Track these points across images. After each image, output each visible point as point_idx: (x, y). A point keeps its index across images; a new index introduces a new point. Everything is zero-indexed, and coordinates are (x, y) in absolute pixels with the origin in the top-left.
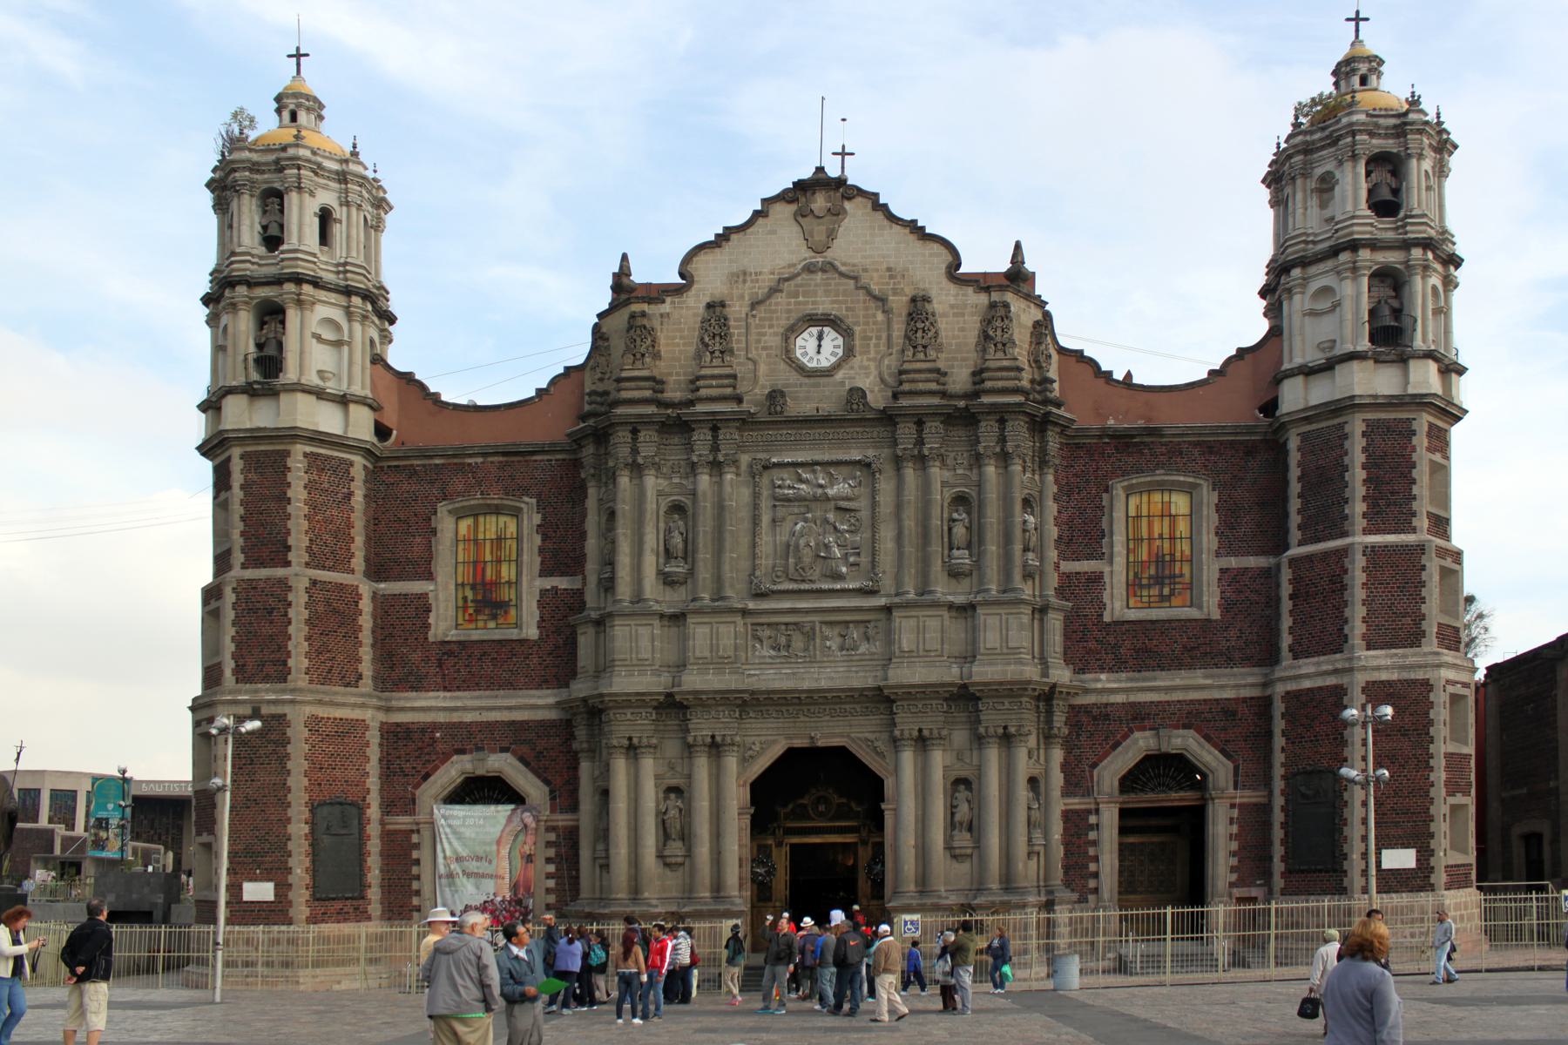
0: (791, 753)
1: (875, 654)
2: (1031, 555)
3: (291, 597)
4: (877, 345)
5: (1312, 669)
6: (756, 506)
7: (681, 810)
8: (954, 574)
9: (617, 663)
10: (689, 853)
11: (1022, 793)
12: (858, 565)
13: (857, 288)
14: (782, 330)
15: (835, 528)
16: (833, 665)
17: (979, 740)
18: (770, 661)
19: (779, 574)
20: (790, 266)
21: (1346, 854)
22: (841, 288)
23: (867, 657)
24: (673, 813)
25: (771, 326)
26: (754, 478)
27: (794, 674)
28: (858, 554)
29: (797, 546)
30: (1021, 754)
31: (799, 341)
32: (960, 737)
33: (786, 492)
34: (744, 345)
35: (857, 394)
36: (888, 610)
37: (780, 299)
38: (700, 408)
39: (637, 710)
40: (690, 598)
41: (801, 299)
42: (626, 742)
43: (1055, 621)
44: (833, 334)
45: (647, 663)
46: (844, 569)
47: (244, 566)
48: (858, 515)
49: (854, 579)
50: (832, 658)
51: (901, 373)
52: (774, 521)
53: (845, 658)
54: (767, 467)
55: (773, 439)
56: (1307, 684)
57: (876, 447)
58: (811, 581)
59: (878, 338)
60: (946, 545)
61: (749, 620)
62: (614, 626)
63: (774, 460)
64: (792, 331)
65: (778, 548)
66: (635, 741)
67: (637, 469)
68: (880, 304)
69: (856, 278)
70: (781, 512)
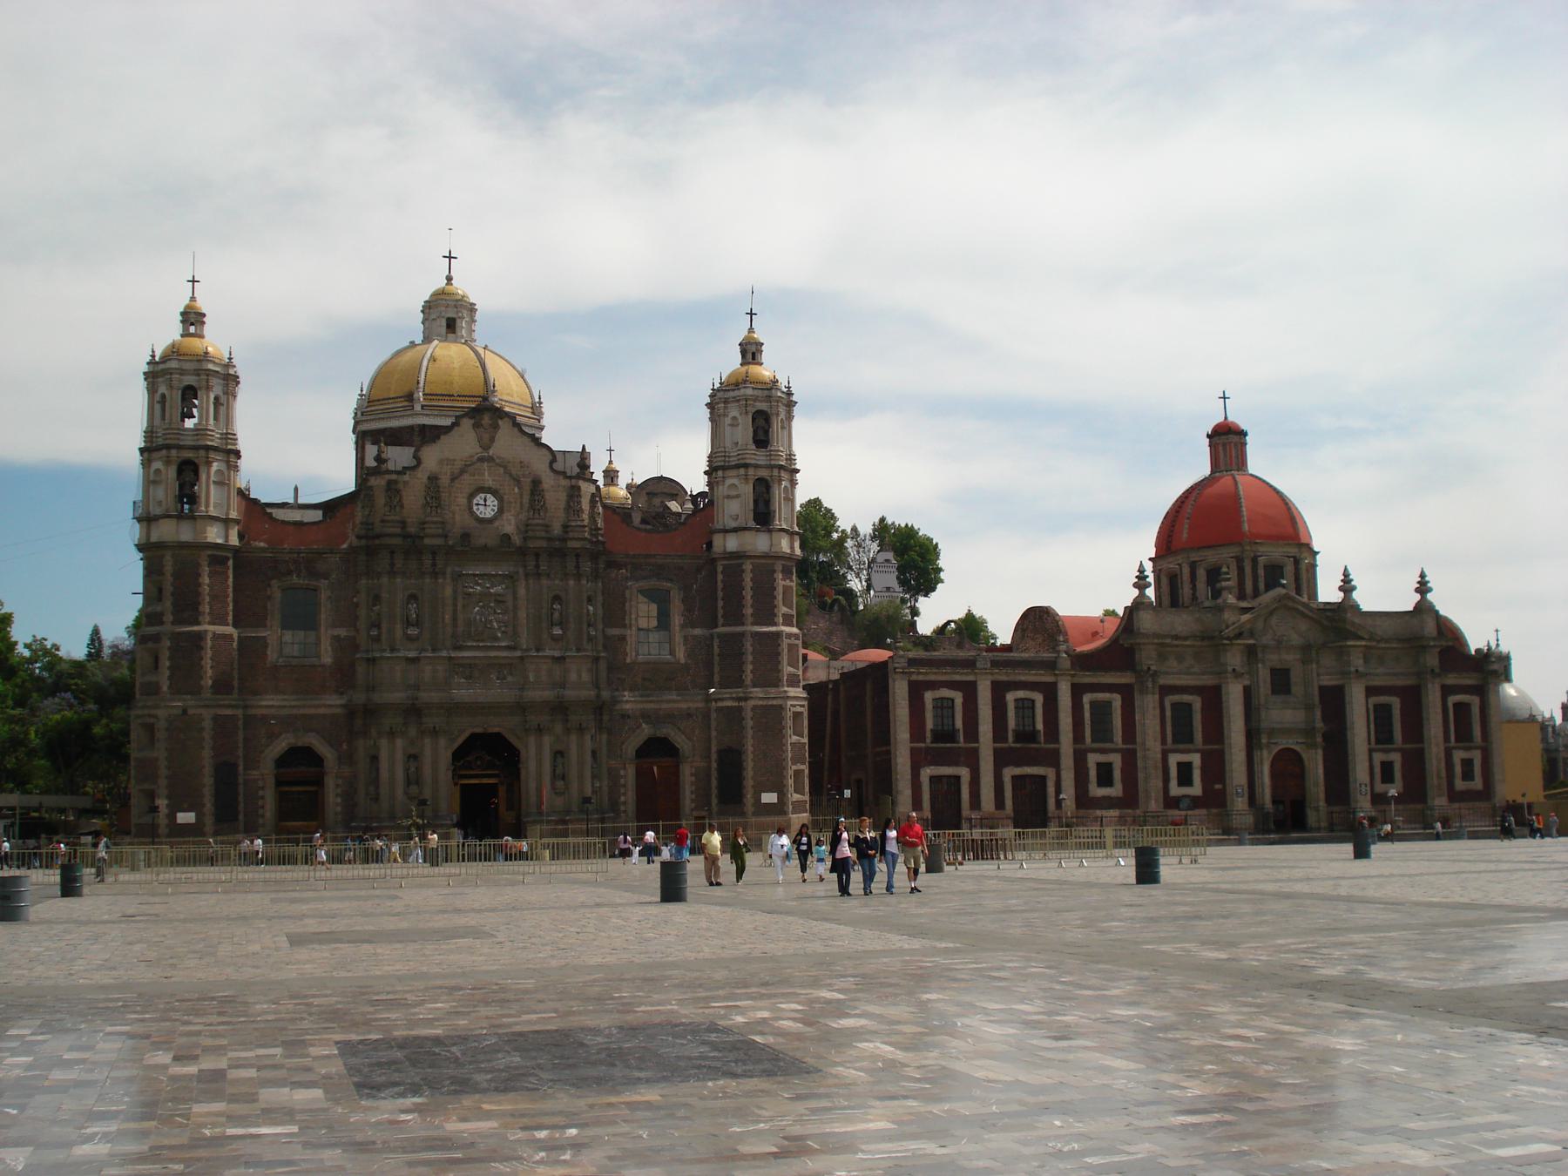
0: (473, 736)
2: (591, 629)
3: (202, 644)
5: (728, 696)
6: (455, 599)
11: (588, 758)
13: (505, 472)
17: (568, 731)
20: (472, 457)
24: (413, 769)
30: (588, 738)
35: (507, 537)
36: (522, 658)
37: (466, 476)
38: (427, 541)
41: (476, 477)
43: (603, 665)
44: (493, 498)
46: (499, 635)
47: (173, 623)
51: (527, 525)
52: (464, 606)
54: (461, 575)
64: (472, 496)
67: (392, 573)
69: (505, 467)
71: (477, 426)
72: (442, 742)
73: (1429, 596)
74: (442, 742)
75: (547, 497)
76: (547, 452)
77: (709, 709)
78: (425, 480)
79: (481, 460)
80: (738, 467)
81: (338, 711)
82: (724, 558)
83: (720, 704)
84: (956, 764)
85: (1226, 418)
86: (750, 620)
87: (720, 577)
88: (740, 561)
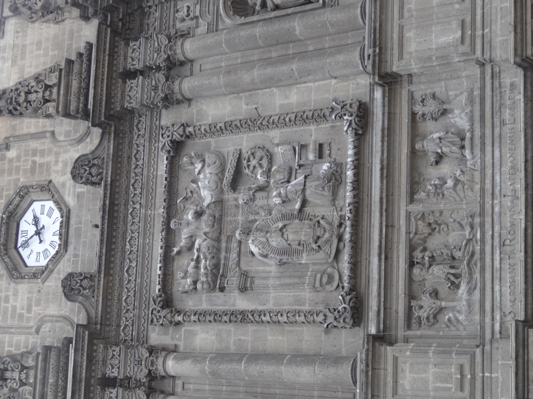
1: (471, 101)
4: (43, 153)
12: (321, 145)
14: (13, 285)
15: (261, 189)
16: (489, 172)
18: (477, 292)
19: (325, 280)
23: (477, 107)
25: (7, 300)
26: (178, 324)
27: (503, 244)
28: (303, 147)
29: (283, 252)
31: (31, 262)
33: (202, 270)
34: (22, 338)
46: (325, 167)
48: (245, 155)
49: (342, 150)
50: (477, 175)
52: (243, 289)
55: (131, 294)
58: (340, 225)
59: (34, 152)
60: (298, 9)
61: (401, 333)
63: (158, 287)
65: (288, 281)
75: (30, 71)
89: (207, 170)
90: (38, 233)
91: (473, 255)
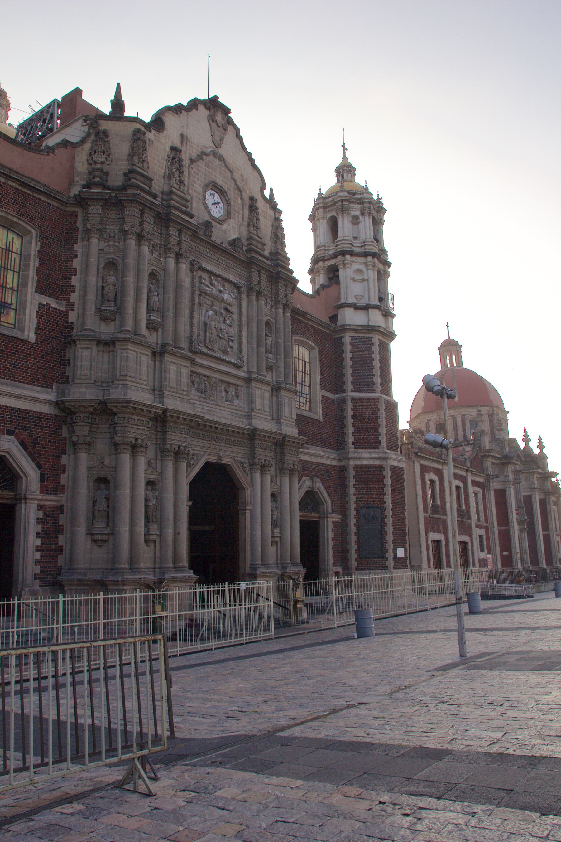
4: (238, 217)
5: (367, 455)
7: (157, 499)
8: (269, 368)
9: (128, 378)
10: (161, 528)
14: (202, 185)
15: (225, 320)
21: (387, 550)
22: (226, 174)
27: (210, 411)
29: (210, 326)
32: (273, 469)
33: (207, 288)
36: (248, 380)
37: (201, 164)
39: (141, 418)
40: (160, 342)
42: (133, 442)
45: (145, 383)
52: (200, 304)
53: (229, 406)
56: (365, 462)
57: (239, 278)
59: (239, 213)
62: (127, 349)
64: (206, 187)
66: (140, 441)
68: (239, 193)
69: (231, 172)
70: (203, 300)
71: (212, 119)
72: (183, 466)
73: (544, 450)
74: (183, 466)
76: (257, 173)
77: (342, 470)
78: (168, 149)
79: (214, 154)
80: (366, 255)
81: (46, 409)
82: (356, 331)
83: (358, 462)
84: (440, 532)
85: (449, 337)
86: (379, 389)
87: (348, 348)
88: (368, 335)
89: (231, 299)
90: (215, 204)
91: (206, 399)
